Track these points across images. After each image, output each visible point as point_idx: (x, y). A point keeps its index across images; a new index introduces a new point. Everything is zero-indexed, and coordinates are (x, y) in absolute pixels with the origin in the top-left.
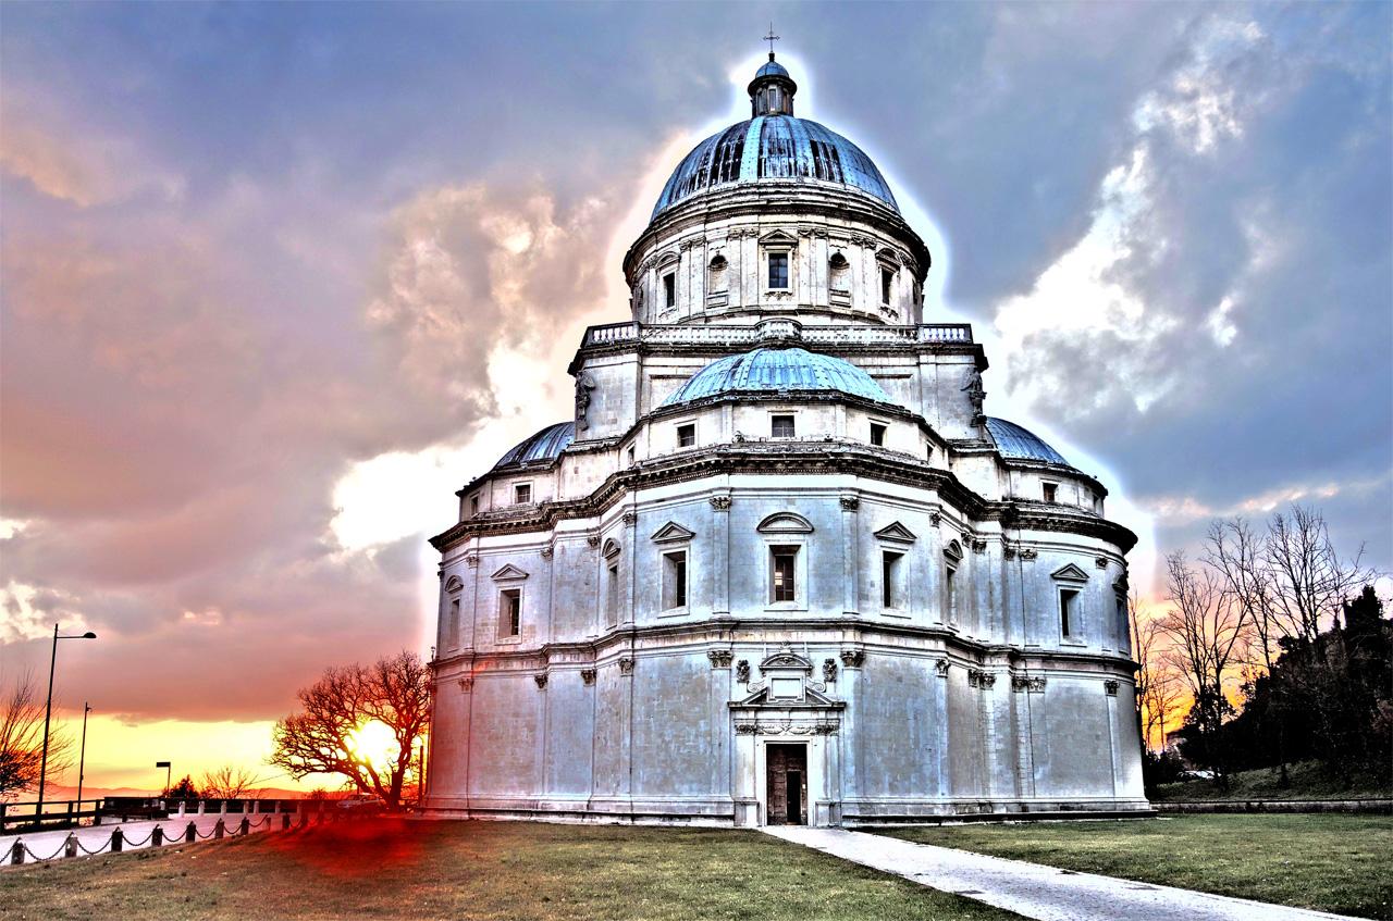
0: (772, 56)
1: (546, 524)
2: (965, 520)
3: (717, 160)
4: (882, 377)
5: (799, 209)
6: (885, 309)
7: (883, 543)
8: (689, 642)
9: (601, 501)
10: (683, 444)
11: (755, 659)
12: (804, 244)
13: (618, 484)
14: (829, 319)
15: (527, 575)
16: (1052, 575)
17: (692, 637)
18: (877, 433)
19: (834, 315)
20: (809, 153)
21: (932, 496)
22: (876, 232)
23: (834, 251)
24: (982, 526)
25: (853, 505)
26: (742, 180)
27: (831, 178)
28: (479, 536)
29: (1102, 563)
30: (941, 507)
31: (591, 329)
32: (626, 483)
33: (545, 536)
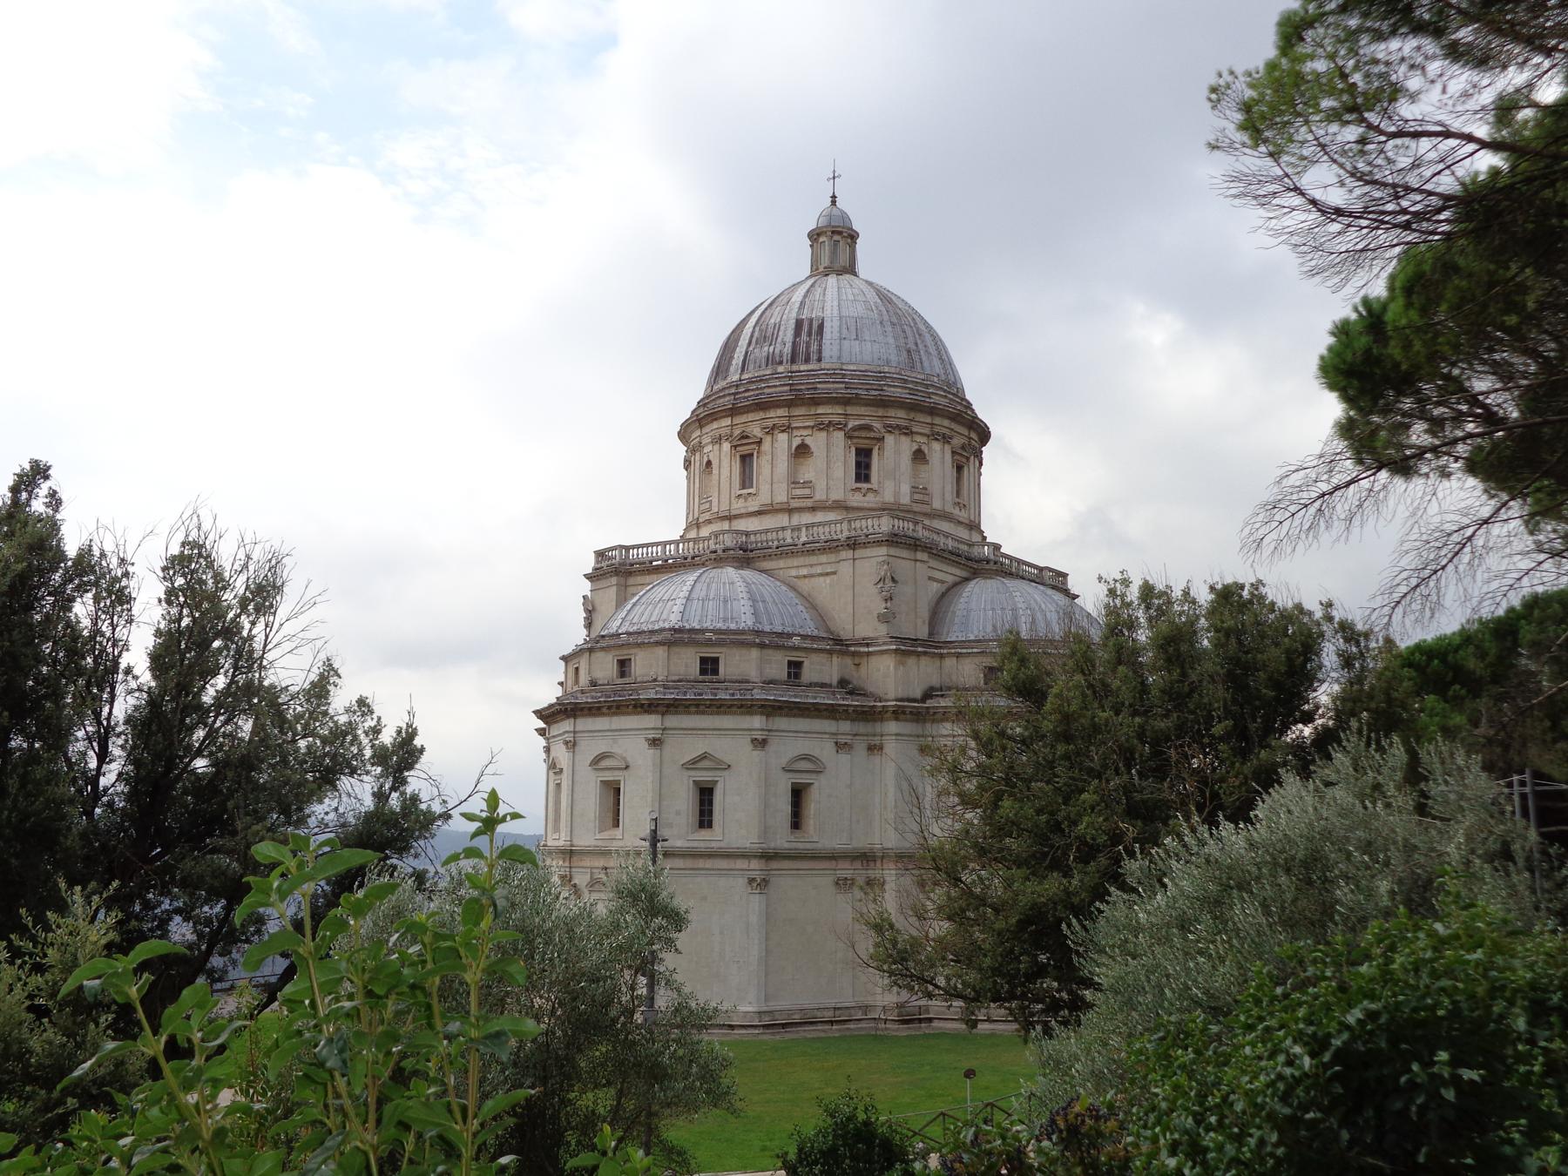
0: (834, 197)
2: (845, 726)
4: (812, 576)
5: (762, 406)
6: (858, 489)
7: (692, 773)
11: (581, 879)
12: (766, 446)
14: (786, 517)
18: (709, 666)
19: (791, 511)
20: (787, 335)
21: (757, 722)
22: (850, 410)
23: (796, 442)
24: (878, 727)
25: (655, 743)
27: (807, 361)
31: (600, 555)
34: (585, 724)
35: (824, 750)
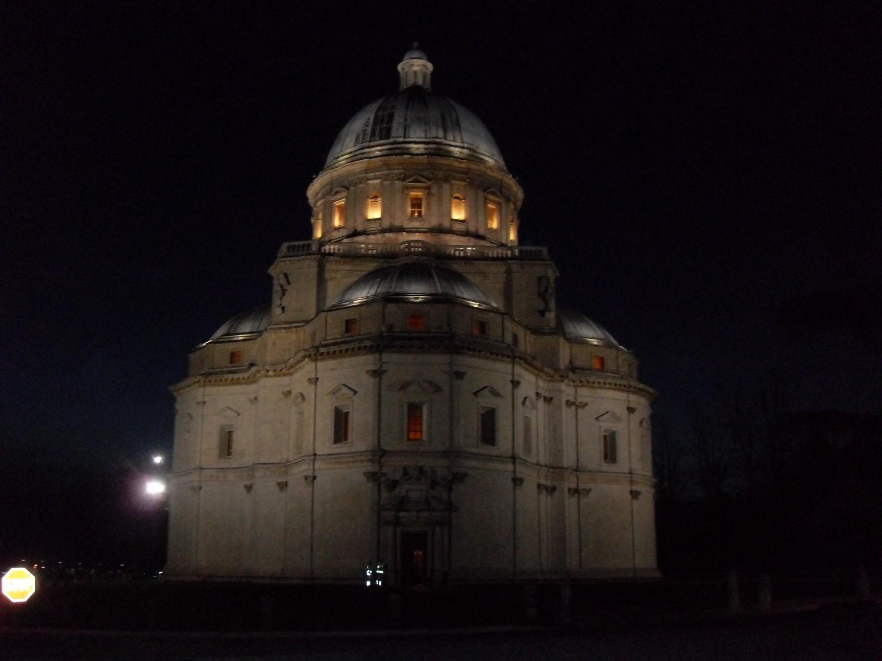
1: (252, 380)
3: (375, 124)
8: (351, 465)
9: (292, 367)
10: (348, 330)
12: (434, 190)
13: (305, 357)
15: (239, 414)
16: (597, 418)
17: (354, 462)
26: (391, 140)
28: (204, 386)
29: (631, 410)
30: (520, 375)
32: (309, 356)
33: (252, 388)
34: (386, 357)
35: (534, 396)
